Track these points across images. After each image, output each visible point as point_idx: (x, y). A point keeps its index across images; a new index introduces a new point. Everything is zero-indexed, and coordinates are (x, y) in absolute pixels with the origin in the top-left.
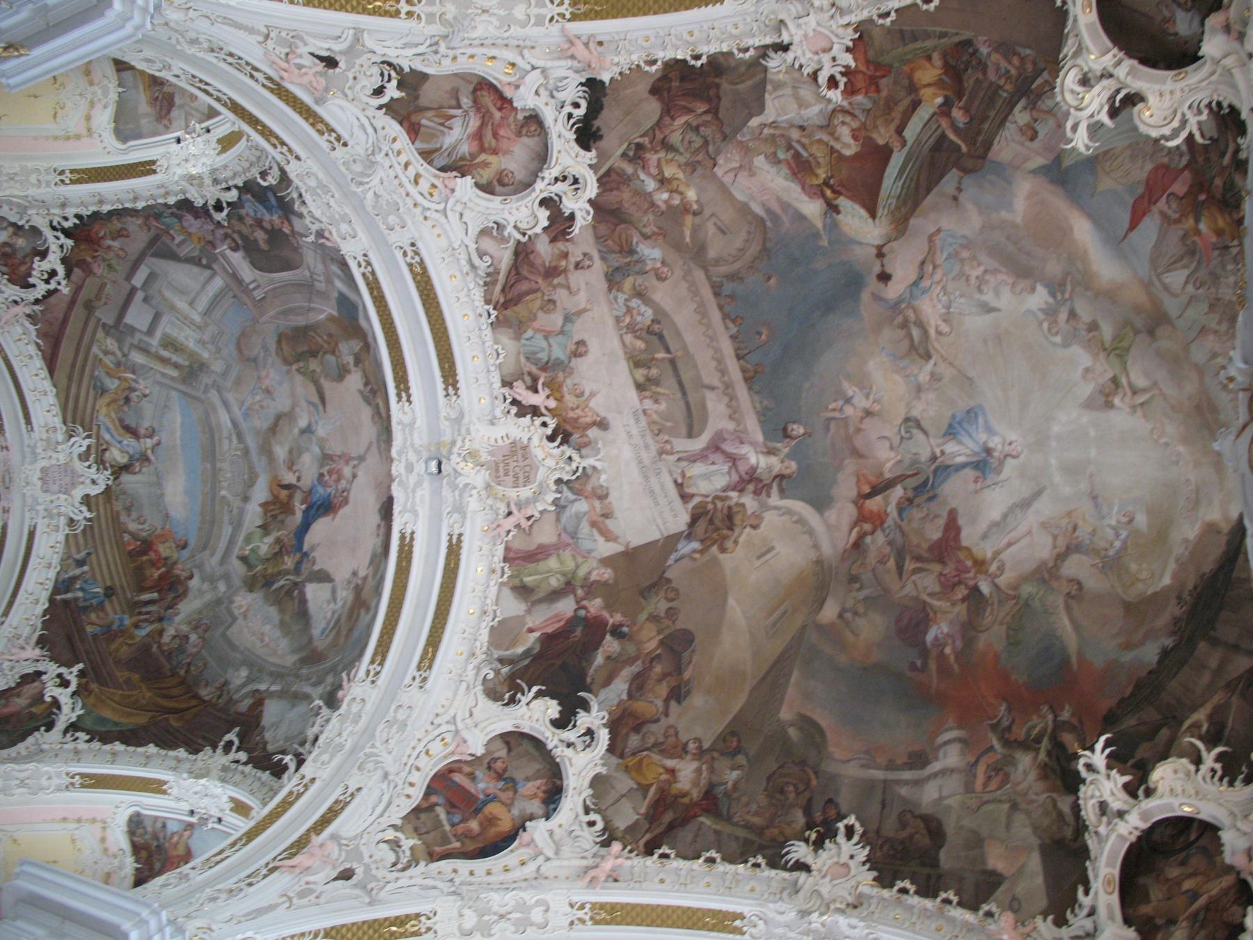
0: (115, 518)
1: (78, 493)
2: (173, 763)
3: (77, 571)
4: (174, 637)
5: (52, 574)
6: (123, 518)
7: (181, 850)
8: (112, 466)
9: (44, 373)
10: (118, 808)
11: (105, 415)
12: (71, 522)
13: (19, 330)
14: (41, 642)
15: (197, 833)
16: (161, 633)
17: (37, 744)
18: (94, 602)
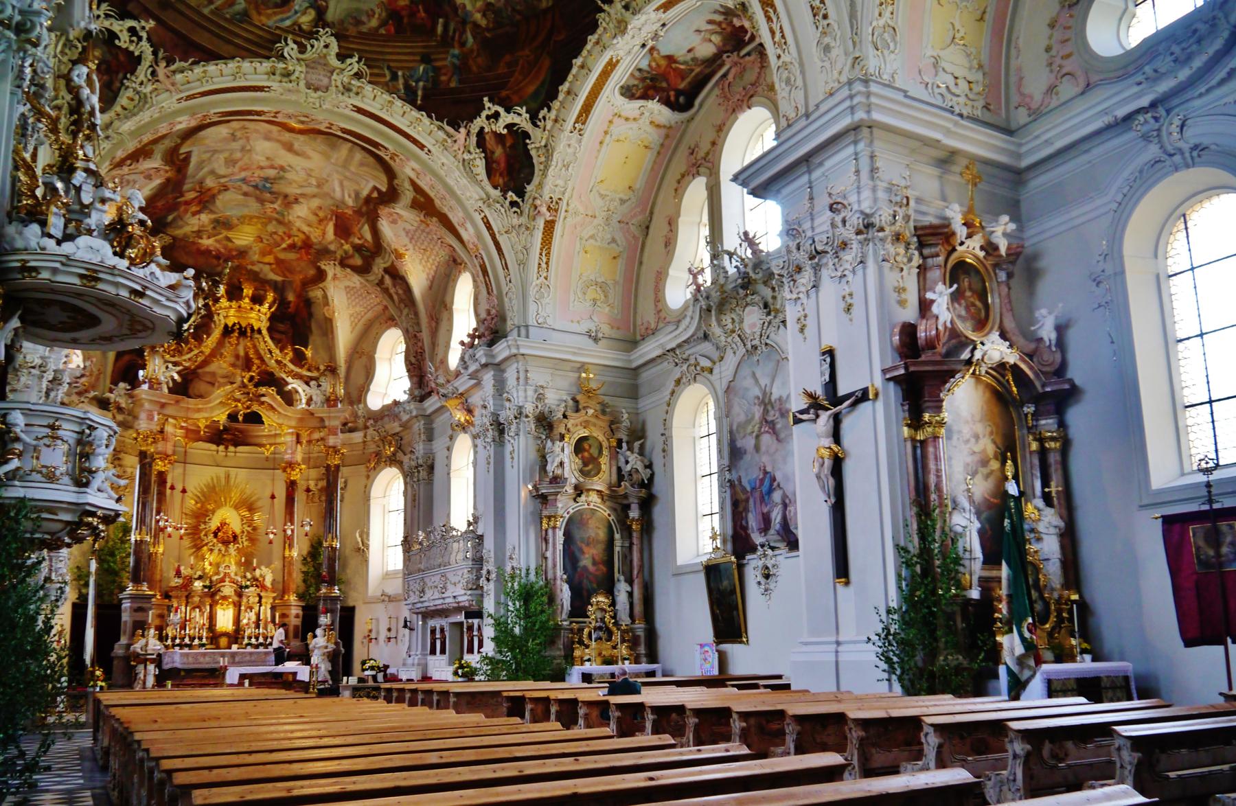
0: (362, 36)
1: (334, 62)
2: (598, 48)
3: (401, 81)
4: (484, 15)
5: (399, 103)
6: (364, 29)
7: (663, 63)
8: (316, 26)
9: (222, 66)
10: (611, 98)
11: (271, 20)
12: (358, 75)
13: (179, 77)
14: (456, 127)
15: (659, 47)
16: (476, 25)
17: (538, 149)
18: (431, 74)
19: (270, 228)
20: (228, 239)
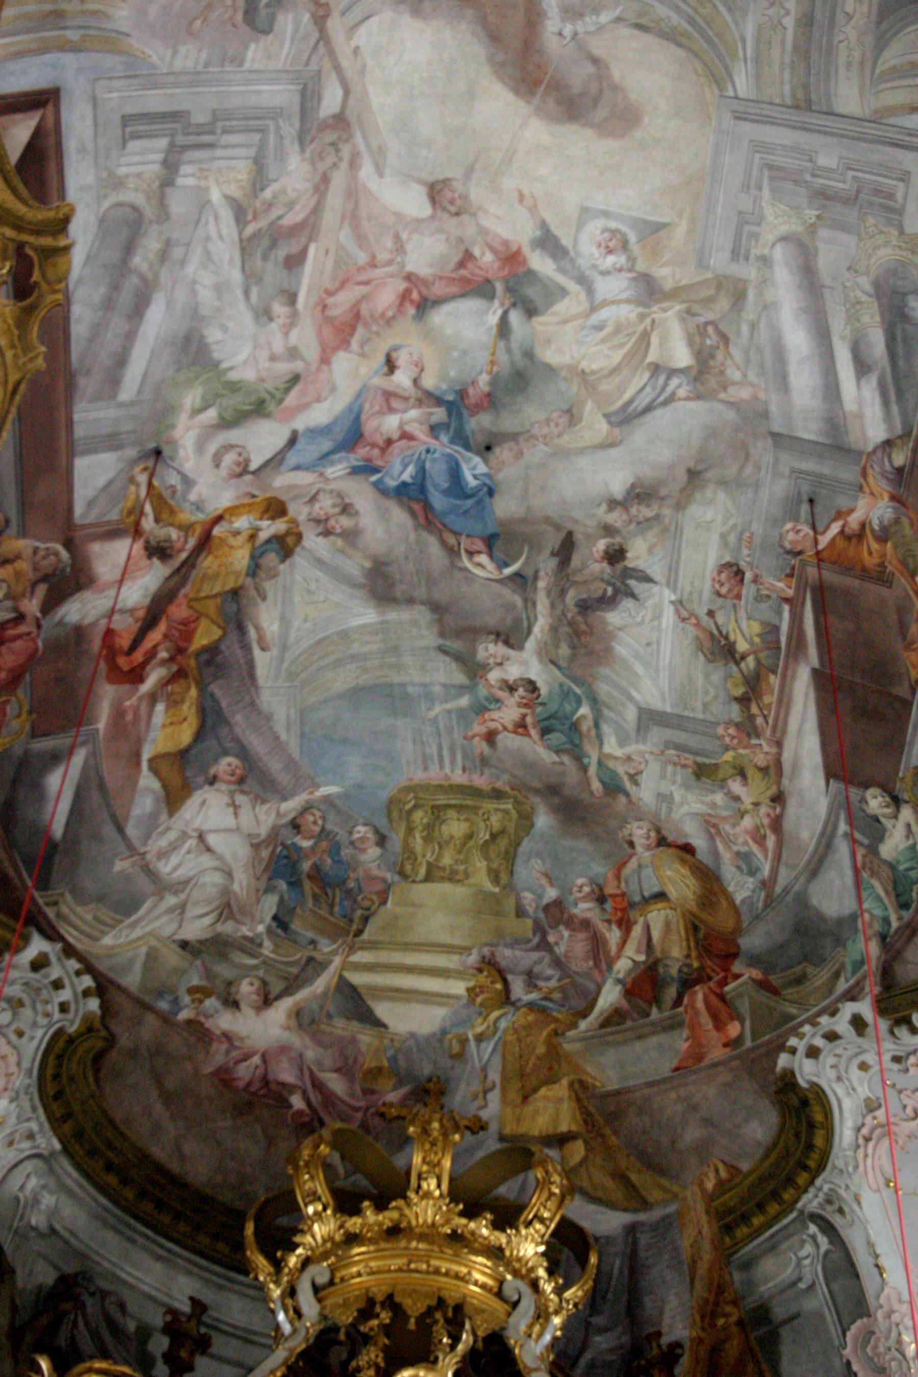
19: (534, 881)
20: (355, 1003)
